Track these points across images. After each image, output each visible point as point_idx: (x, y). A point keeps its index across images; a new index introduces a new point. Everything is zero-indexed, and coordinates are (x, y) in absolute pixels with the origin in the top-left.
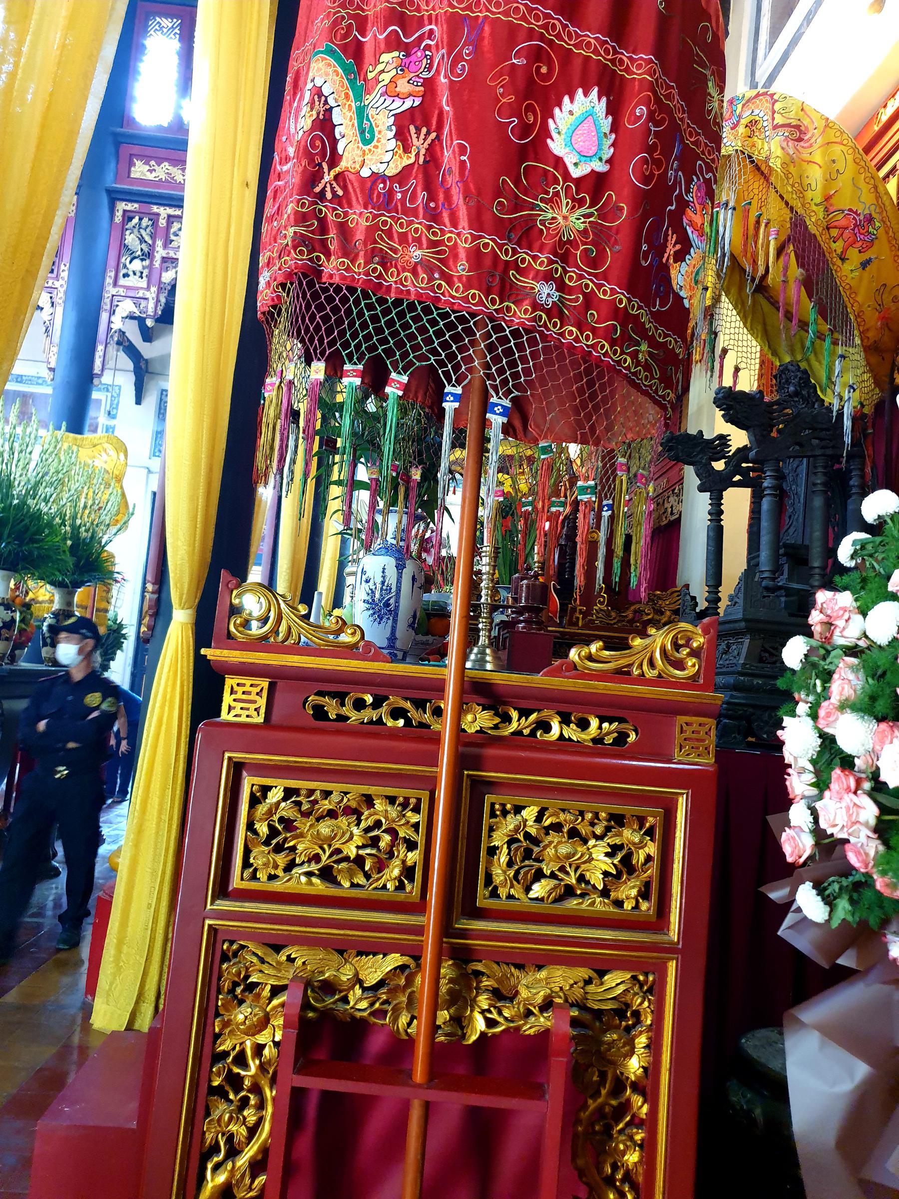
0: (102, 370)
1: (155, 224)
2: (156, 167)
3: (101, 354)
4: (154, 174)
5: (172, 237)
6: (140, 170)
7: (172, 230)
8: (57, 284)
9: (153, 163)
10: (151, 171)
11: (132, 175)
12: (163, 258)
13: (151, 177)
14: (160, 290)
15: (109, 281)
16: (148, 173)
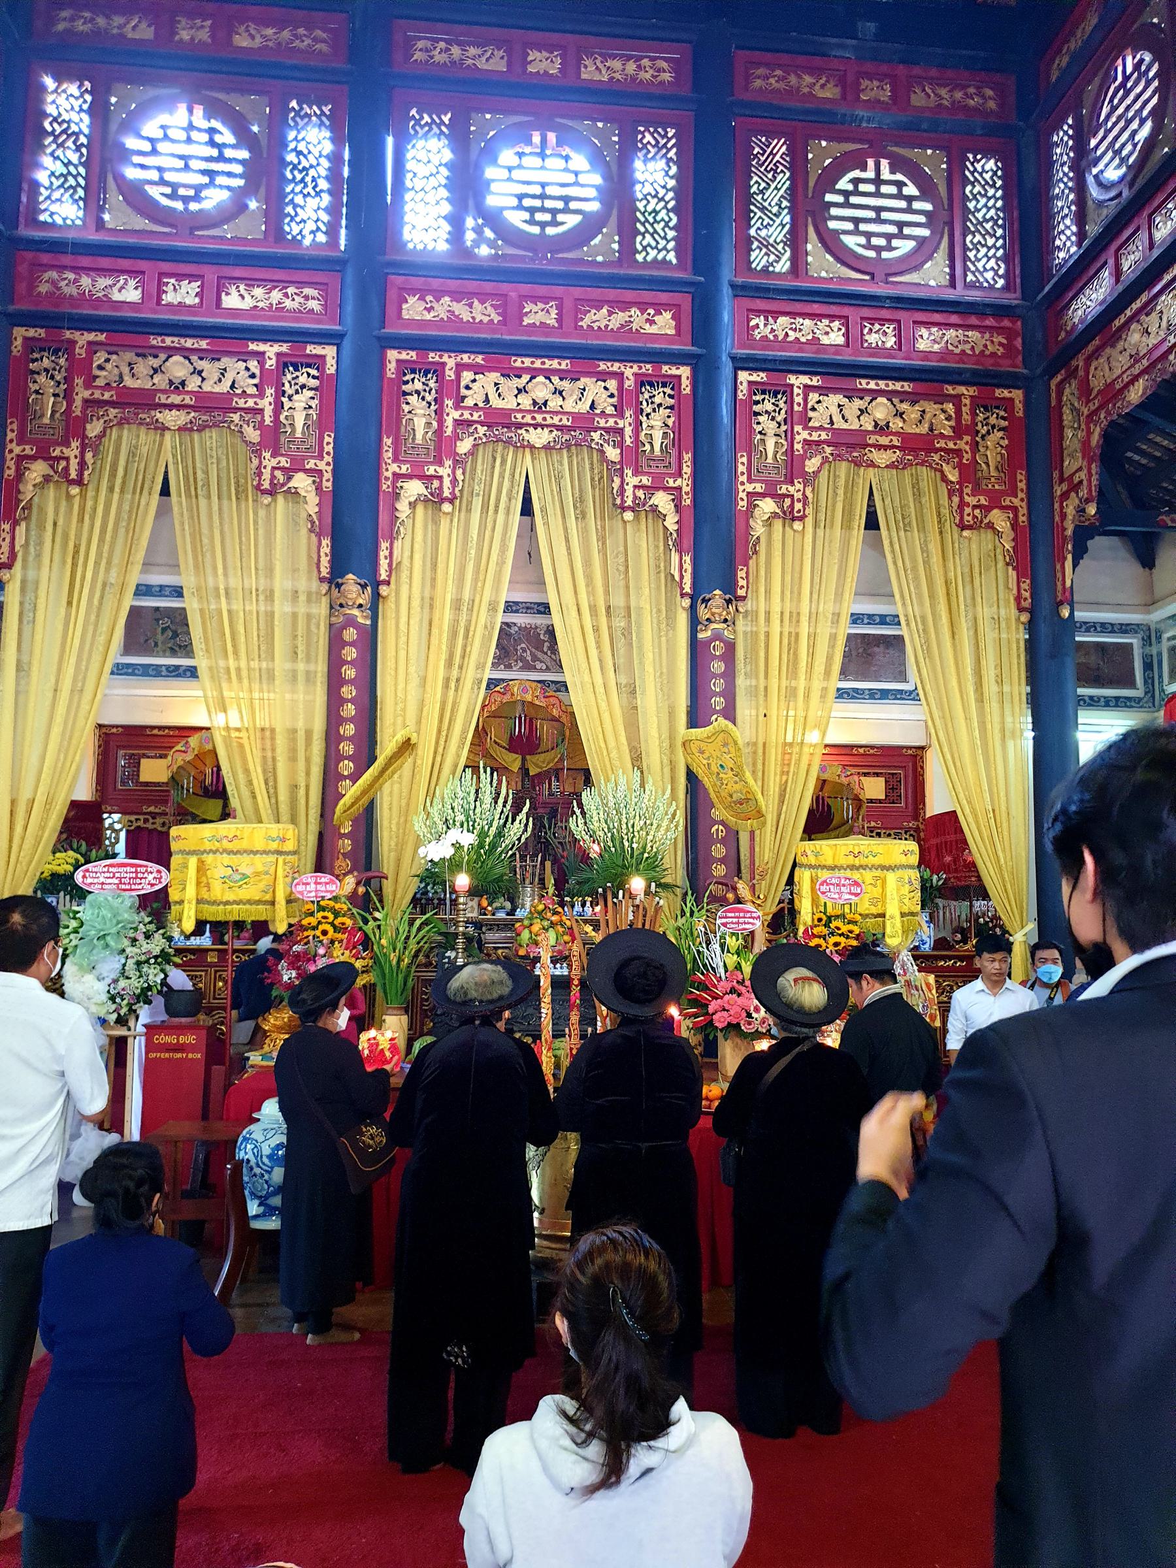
0: (389, 576)
1: (440, 378)
2: (435, 305)
3: (387, 553)
4: (432, 314)
5: (464, 392)
6: (413, 309)
7: (463, 384)
8: (322, 465)
9: (429, 298)
10: (429, 310)
11: (405, 315)
12: (455, 420)
13: (428, 316)
14: (456, 462)
15: (388, 455)
16: (425, 312)
